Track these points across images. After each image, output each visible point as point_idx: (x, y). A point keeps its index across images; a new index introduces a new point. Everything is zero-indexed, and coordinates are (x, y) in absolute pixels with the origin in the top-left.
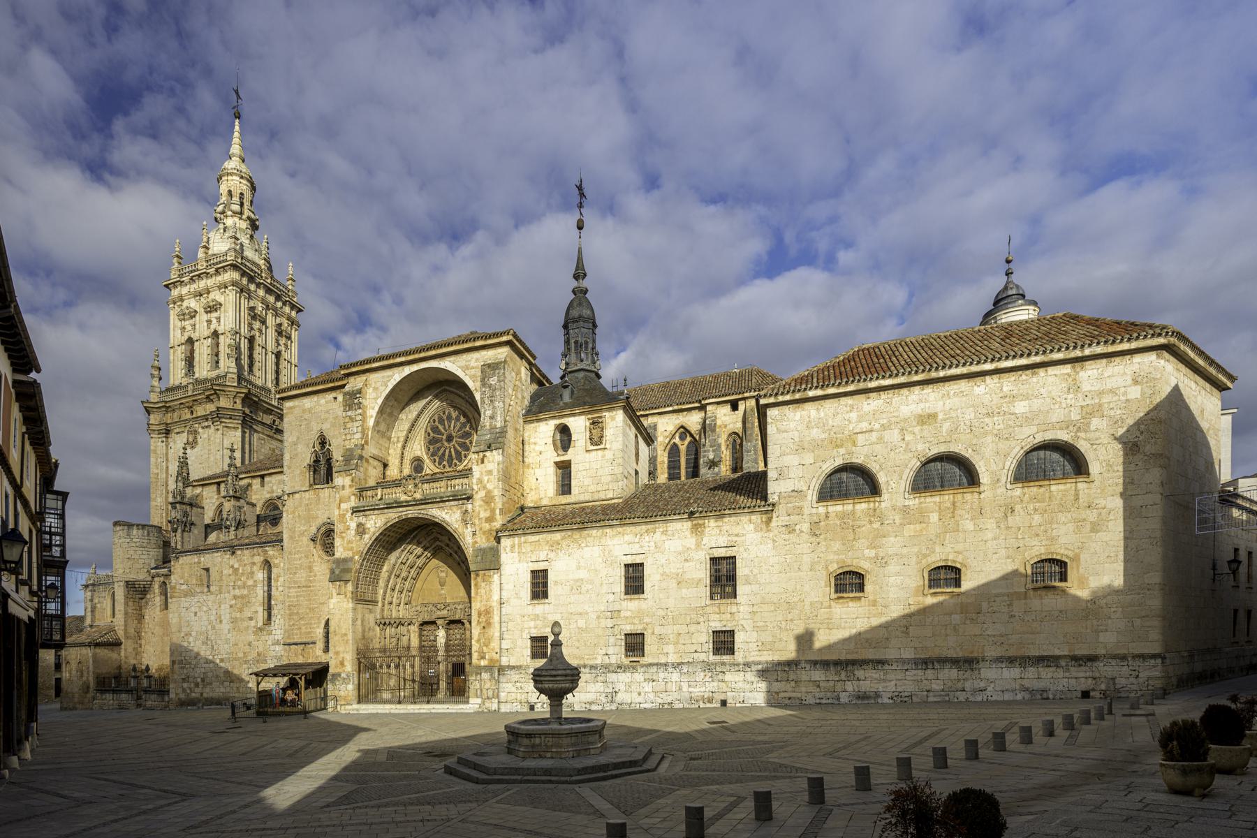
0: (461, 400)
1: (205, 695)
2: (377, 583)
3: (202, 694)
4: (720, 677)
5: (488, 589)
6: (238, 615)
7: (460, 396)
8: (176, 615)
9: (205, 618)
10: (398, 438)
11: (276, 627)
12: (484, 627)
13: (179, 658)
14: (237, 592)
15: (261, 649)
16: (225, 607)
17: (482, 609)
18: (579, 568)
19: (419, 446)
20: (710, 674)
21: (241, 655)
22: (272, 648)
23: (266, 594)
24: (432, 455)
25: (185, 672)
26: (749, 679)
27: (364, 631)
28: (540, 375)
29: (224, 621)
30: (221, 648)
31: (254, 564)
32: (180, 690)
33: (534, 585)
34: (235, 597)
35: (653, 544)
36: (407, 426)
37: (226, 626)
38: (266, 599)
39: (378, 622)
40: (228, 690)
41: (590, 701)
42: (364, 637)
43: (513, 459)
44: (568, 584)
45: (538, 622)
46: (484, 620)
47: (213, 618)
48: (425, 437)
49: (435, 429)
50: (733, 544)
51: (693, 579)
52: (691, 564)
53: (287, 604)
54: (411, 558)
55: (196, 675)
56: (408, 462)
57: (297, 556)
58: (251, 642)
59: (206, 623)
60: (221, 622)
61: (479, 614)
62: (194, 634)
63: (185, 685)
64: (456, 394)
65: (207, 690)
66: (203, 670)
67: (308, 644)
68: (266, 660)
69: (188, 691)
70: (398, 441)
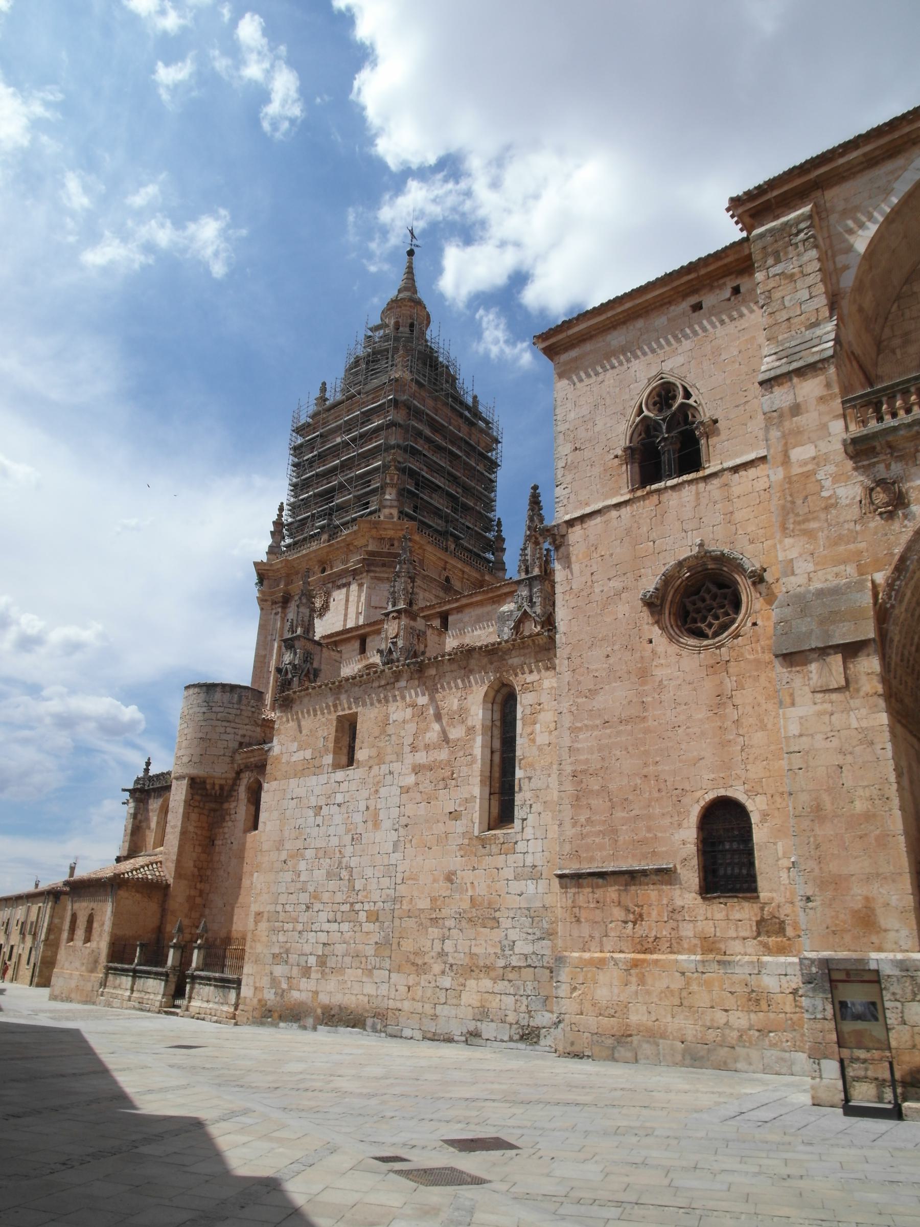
1: (324, 999)
3: (316, 993)
6: (422, 809)
8: (275, 814)
9: (338, 819)
11: (529, 833)
13: (271, 908)
14: (421, 757)
15: (481, 890)
16: (389, 792)
21: (424, 904)
22: (516, 887)
23: (497, 758)
25: (282, 938)
29: (387, 824)
30: (373, 886)
32: (265, 982)
34: (417, 769)
37: (384, 838)
40: (384, 990)
47: (358, 818)
53: (569, 769)
55: (307, 949)
58: (454, 873)
59: (341, 830)
60: (377, 824)
63: (279, 970)
65: (331, 984)
66: (323, 937)
69: (284, 986)
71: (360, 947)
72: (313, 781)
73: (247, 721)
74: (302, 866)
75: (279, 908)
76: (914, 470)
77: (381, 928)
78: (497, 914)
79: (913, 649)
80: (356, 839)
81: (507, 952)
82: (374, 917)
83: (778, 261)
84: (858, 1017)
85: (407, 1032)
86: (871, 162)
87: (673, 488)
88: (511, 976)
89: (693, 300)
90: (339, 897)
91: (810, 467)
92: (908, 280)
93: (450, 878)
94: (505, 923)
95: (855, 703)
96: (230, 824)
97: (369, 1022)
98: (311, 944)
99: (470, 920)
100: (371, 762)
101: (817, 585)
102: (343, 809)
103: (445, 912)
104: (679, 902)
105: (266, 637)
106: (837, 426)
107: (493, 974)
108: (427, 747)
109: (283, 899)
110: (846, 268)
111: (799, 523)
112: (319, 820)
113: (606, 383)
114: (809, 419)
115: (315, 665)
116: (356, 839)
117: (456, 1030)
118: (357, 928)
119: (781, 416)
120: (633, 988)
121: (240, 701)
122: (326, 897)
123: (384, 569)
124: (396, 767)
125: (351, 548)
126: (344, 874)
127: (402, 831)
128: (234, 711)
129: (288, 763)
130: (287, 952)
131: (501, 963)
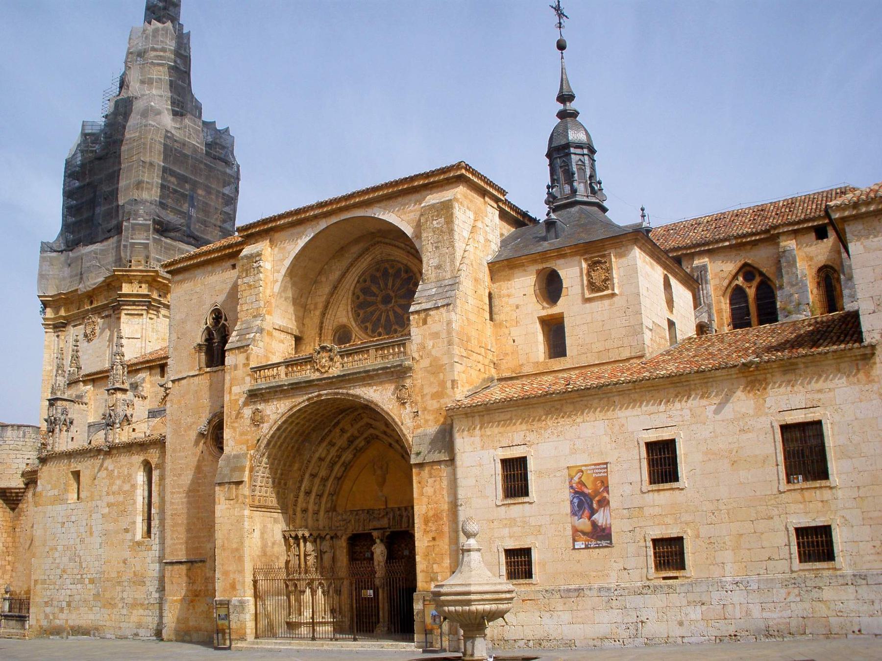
0: (402, 251)
1: (71, 623)
2: (285, 484)
3: (67, 620)
4: (815, 594)
5: (438, 487)
6: (111, 526)
7: (398, 247)
9: (72, 530)
10: (316, 304)
12: (434, 539)
13: (42, 577)
14: (111, 499)
15: (138, 568)
17: (431, 513)
18: (574, 451)
19: (344, 313)
20: (796, 591)
21: (114, 575)
23: (146, 500)
24: (362, 322)
25: (49, 593)
26: (866, 597)
27: (264, 547)
28: (511, 208)
29: (96, 534)
31: (132, 465)
33: (506, 478)
34: (109, 505)
35: (688, 412)
36: (326, 289)
37: (96, 540)
38: (146, 507)
39: (287, 534)
40: (98, 616)
41: (600, 636)
42: (264, 553)
43: (473, 317)
44: (558, 474)
45: (515, 529)
46: (434, 528)
47: (82, 530)
48: (353, 301)
49: (366, 291)
50: (815, 403)
51: (756, 456)
52: (750, 435)
55: (62, 598)
56: (330, 332)
57: (182, 454)
59: (75, 536)
60: (91, 534)
61: (426, 521)
62: (60, 548)
64: (395, 246)
65: (74, 616)
66: (69, 592)
67: (196, 562)
68: (144, 582)
70: (316, 308)
71: (87, 597)
72: (59, 508)
73: (30, 449)
74: (57, 555)
75: (46, 577)
76: (267, 407)
77: (95, 586)
78: (145, 580)
80: (82, 541)
81: (149, 597)
82: (92, 581)
83: (247, 276)
84: (223, 619)
85: (108, 636)
86: (293, 225)
87: (215, 372)
88: (150, 608)
89: (232, 262)
90: (76, 571)
91: (237, 397)
92: (320, 273)
93: (125, 562)
94: (148, 583)
95: (237, 506)
96: (24, 518)
97: (92, 632)
98: (63, 595)
99: (134, 582)
100: (87, 500)
101: (235, 452)
102: (75, 525)
103: (124, 578)
104: (208, 575)
105: (50, 356)
106: (248, 379)
107: (143, 607)
108: (114, 493)
109: (48, 573)
110: (277, 281)
111: (231, 423)
112: (64, 530)
113: (193, 301)
114: (240, 372)
115: (69, 416)
116: (82, 541)
117: (128, 633)
118: (84, 587)
119: (231, 369)
120: (191, 611)
121: (24, 436)
122: (69, 571)
123: (134, 307)
124: (99, 503)
125: (111, 287)
126: (77, 559)
127: (104, 538)
128: (21, 443)
129: (46, 496)
130: (52, 600)
131: (146, 602)
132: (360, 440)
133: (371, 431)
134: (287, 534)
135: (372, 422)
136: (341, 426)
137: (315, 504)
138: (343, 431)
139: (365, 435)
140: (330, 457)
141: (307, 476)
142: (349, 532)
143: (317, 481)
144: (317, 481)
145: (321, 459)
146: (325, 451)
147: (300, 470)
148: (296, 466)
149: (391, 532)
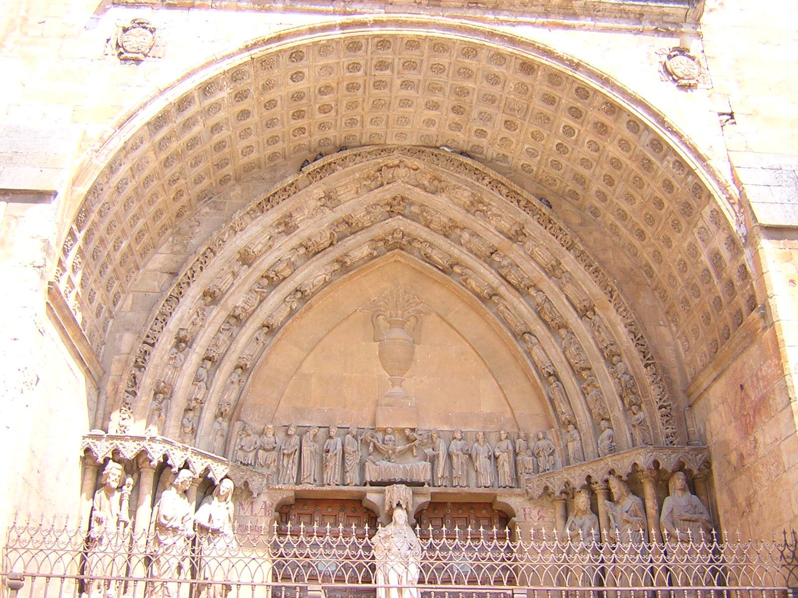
39: (102, 450)
54: (285, 246)
79: (118, 256)
132: (360, 237)
133: (397, 222)
134: (102, 450)
135: (418, 195)
136: (330, 179)
137: (197, 379)
138: (330, 199)
139: (377, 231)
140: (269, 260)
141: (194, 292)
142: (287, 489)
143: (217, 316)
144: (217, 316)
145: (246, 258)
146: (264, 239)
147: (174, 274)
148: (160, 259)
149: (433, 495)
